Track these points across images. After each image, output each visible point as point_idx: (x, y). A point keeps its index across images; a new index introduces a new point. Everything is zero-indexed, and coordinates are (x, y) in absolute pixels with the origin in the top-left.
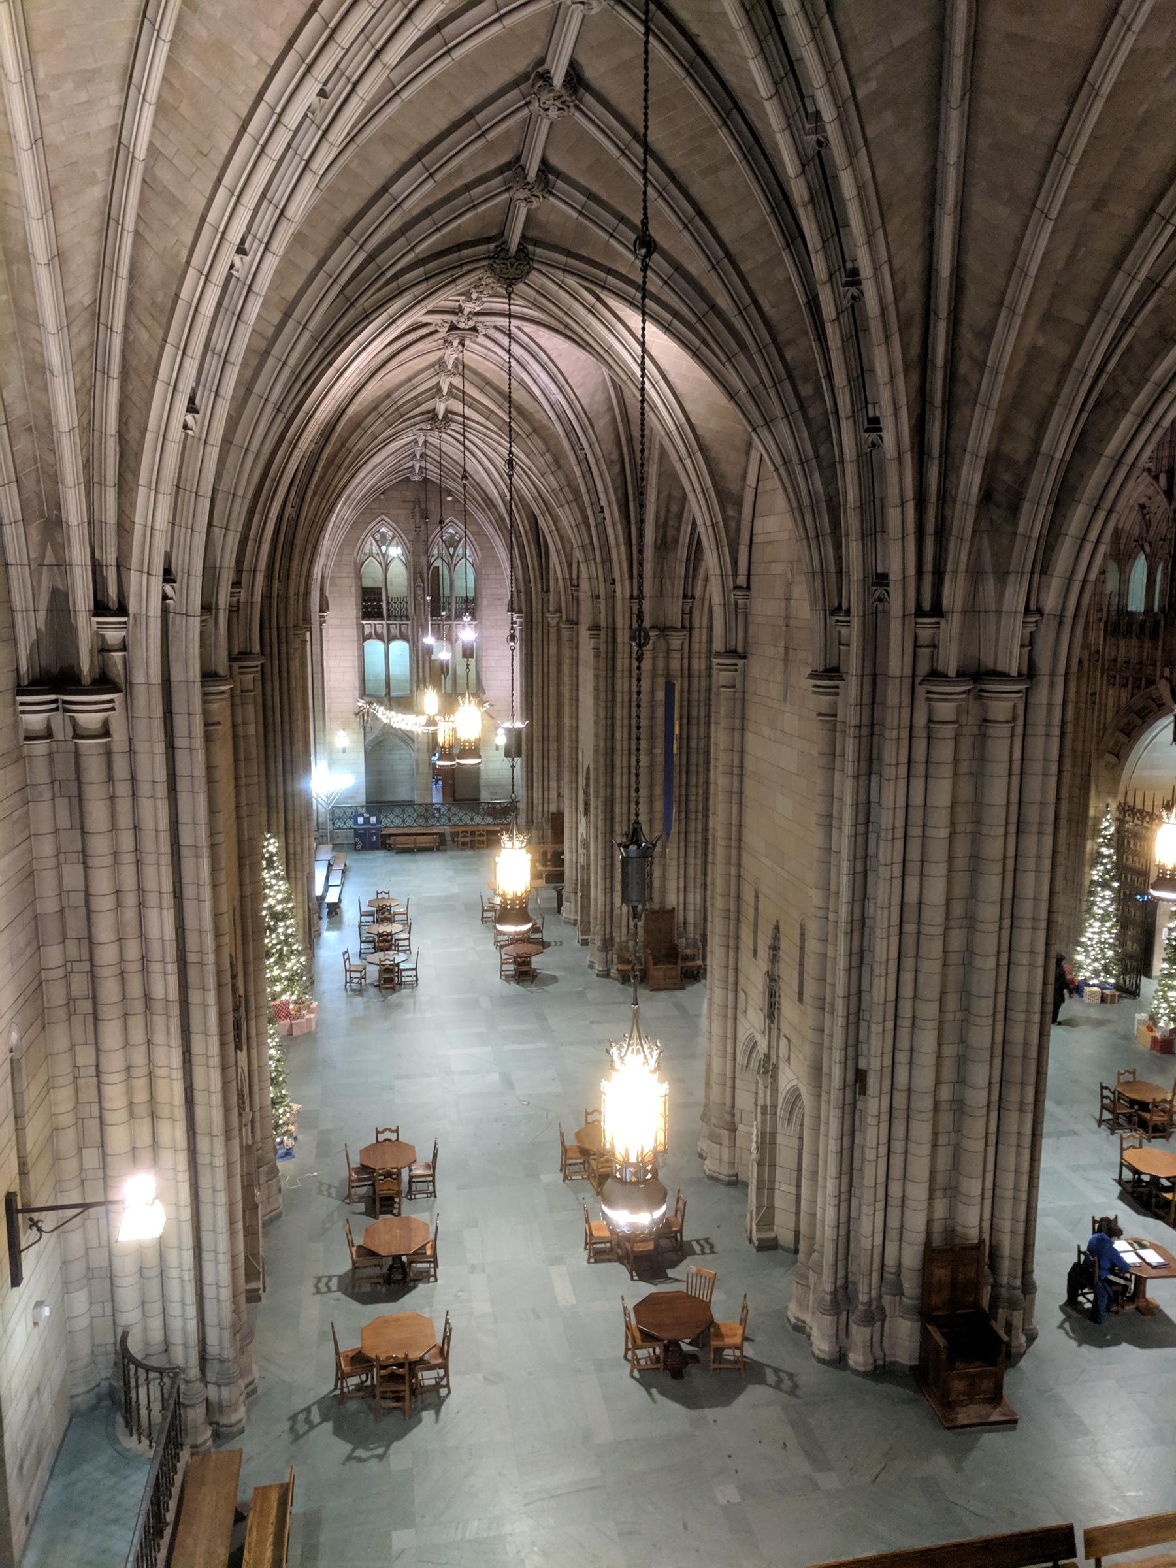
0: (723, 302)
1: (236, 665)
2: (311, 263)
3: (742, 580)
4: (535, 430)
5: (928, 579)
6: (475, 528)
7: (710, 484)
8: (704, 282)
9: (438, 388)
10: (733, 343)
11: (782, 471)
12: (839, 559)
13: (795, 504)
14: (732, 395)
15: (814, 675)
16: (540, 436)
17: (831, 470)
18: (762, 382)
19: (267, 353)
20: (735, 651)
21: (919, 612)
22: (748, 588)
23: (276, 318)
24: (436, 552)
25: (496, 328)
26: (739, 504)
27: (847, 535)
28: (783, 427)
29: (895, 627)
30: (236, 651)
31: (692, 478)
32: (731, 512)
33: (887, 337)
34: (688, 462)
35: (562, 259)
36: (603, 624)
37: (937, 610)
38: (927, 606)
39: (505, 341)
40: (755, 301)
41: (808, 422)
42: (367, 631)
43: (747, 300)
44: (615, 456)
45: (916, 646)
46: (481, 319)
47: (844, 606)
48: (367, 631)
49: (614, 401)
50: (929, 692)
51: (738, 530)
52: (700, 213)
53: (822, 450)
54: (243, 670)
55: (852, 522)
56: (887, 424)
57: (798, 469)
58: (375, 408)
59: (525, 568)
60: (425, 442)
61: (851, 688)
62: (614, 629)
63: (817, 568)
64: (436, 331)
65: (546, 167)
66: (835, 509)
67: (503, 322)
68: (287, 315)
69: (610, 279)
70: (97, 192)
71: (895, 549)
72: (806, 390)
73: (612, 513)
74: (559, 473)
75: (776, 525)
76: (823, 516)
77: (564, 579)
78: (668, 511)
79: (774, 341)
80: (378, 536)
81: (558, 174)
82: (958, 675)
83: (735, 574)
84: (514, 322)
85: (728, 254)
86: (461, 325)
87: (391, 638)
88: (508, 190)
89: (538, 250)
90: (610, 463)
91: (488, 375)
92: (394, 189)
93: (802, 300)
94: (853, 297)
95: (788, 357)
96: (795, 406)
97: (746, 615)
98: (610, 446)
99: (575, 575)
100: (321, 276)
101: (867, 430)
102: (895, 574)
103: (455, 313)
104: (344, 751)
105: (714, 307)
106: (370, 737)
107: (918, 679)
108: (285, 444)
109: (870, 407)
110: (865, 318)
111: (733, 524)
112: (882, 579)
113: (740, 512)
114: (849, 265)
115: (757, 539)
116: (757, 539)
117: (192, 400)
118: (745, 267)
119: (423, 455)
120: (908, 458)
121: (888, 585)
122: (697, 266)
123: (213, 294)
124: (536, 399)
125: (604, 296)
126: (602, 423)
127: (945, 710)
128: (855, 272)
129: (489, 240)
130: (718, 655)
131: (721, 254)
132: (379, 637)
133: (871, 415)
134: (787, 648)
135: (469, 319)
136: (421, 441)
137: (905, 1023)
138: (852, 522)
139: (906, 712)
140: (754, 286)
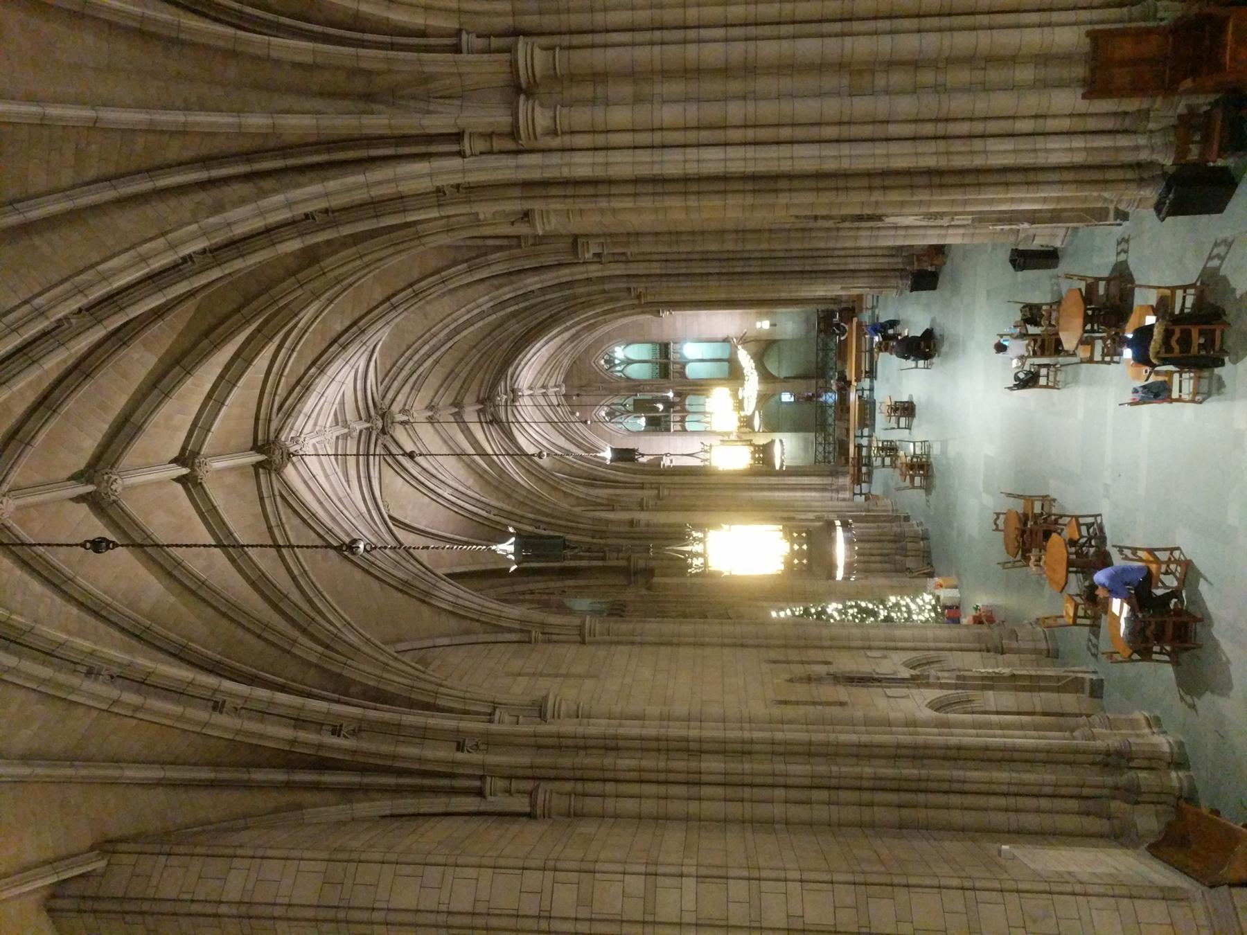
1: (587, 640)
3: (514, 242)
21: (461, 154)
30: (578, 638)
37: (458, 137)
38: (455, 148)
42: (678, 427)
45: (491, 152)
65: (179, 460)
81: (184, 449)
89: (260, 437)
129: (257, 475)
130: (577, 257)
132: (683, 420)
137: (846, 132)
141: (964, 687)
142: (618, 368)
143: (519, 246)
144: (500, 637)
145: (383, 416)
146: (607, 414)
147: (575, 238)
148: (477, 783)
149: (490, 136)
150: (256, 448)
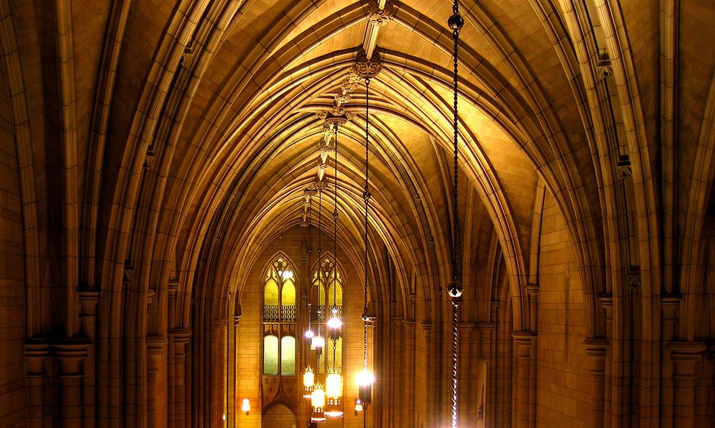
0: (514, 82)
2: (234, 59)
3: (532, 279)
4: (385, 186)
5: (669, 270)
6: (344, 258)
7: (508, 212)
8: (500, 70)
9: (319, 159)
10: (522, 109)
11: (559, 196)
12: (602, 257)
13: (569, 219)
14: (522, 145)
15: (588, 341)
16: (388, 189)
17: (595, 198)
18: (544, 135)
19: (202, 118)
20: (530, 330)
21: (664, 293)
22: (538, 284)
23: (209, 95)
24: (316, 275)
25: (358, 115)
26: (530, 225)
27: (608, 239)
28: (559, 165)
29: (646, 304)
30: (173, 326)
31: (494, 207)
32: (523, 232)
33: (631, 100)
34: (492, 197)
35: (402, 59)
36: (433, 319)
37: (677, 292)
38: (669, 289)
39: (363, 124)
40: (536, 80)
41: (577, 162)
43: (531, 79)
44: (441, 202)
45: (662, 319)
46: (349, 109)
47: (608, 290)
48: (266, 329)
49: (441, 165)
50: (673, 353)
51: (529, 244)
52: (496, 23)
53: (588, 180)
54: (177, 339)
55: (610, 228)
56: (634, 158)
57: (570, 194)
58: (276, 173)
59: (378, 284)
60: (310, 200)
61: (615, 350)
62: (441, 323)
63: (587, 263)
64: (319, 119)
66: (598, 220)
67: (363, 111)
68: (216, 94)
69: (436, 71)
70: (101, 19)
71: (643, 248)
72: (575, 139)
73: (440, 243)
74: (403, 215)
75: (557, 239)
76: (589, 227)
77: (405, 289)
78: (479, 240)
79: (551, 106)
80: (276, 264)
82: (696, 339)
83: (528, 275)
84: (371, 111)
85: (516, 49)
86: (335, 114)
88: (366, 15)
89: (386, 55)
90: (438, 208)
91: (353, 149)
92: (290, 13)
93: (569, 77)
94: (606, 74)
95: (561, 117)
96: (567, 149)
97: (536, 304)
98: (438, 195)
99: (413, 287)
100: (240, 68)
101: (620, 164)
102: (644, 266)
103: (332, 106)
104: (247, 414)
105: (508, 85)
106: (266, 404)
107: (665, 343)
108: (213, 186)
109: (621, 149)
110: (615, 86)
111: (525, 239)
112: (635, 270)
113: (530, 231)
114: (601, 52)
115: (543, 250)
116: (543, 250)
117: (150, 147)
118: (528, 58)
119: (309, 209)
120: (650, 182)
121: (640, 274)
122: (494, 59)
123: (169, 78)
124: (386, 164)
125: (431, 83)
126: (433, 180)
127: (687, 367)
128: (606, 56)
130: (517, 333)
131: (511, 49)
132: (275, 334)
133: (622, 154)
134: (567, 325)
135: (341, 110)
136: (308, 199)
138: (610, 228)
139: (656, 367)
140: (536, 70)
142: (321, 275)
143: (528, 284)
145: (344, 117)
147: (535, 334)
148: (91, 281)
149: (676, 319)
150: (378, 49)
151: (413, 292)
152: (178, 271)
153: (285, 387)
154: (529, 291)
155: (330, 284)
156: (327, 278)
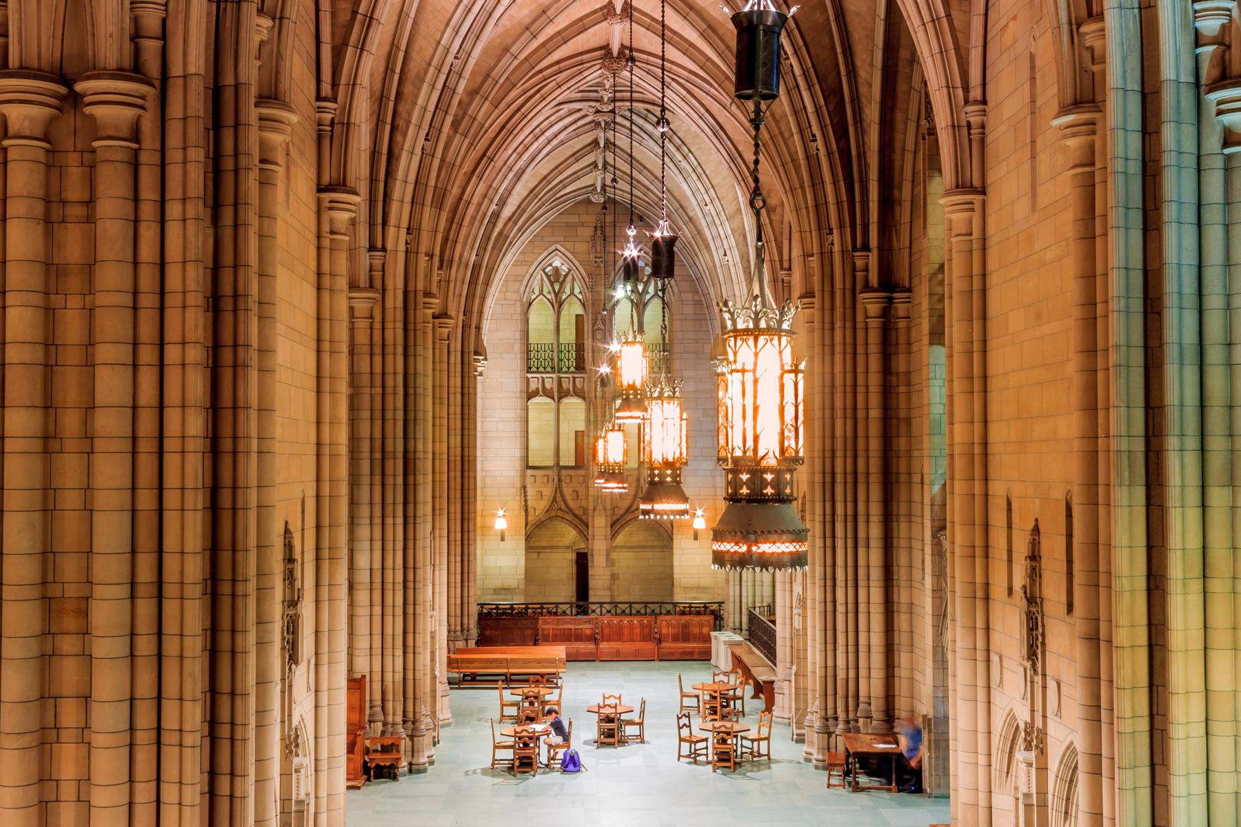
3: (976, 93)
30: (326, 180)
42: (533, 387)
83: (966, 89)
87: (563, 394)
97: (983, 142)
99: (786, 257)
132: (548, 393)
141: (285, 812)
143: (967, 102)
144: (326, 51)
146: (557, 270)
147: (983, 192)
151: (786, 265)
152: (335, 85)
153: (567, 491)
154: (971, 114)
155: (645, 305)
156: (641, 295)
